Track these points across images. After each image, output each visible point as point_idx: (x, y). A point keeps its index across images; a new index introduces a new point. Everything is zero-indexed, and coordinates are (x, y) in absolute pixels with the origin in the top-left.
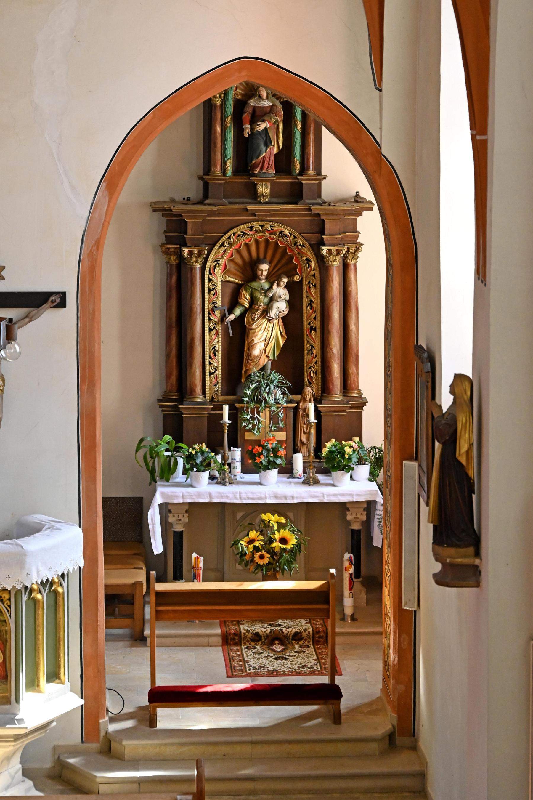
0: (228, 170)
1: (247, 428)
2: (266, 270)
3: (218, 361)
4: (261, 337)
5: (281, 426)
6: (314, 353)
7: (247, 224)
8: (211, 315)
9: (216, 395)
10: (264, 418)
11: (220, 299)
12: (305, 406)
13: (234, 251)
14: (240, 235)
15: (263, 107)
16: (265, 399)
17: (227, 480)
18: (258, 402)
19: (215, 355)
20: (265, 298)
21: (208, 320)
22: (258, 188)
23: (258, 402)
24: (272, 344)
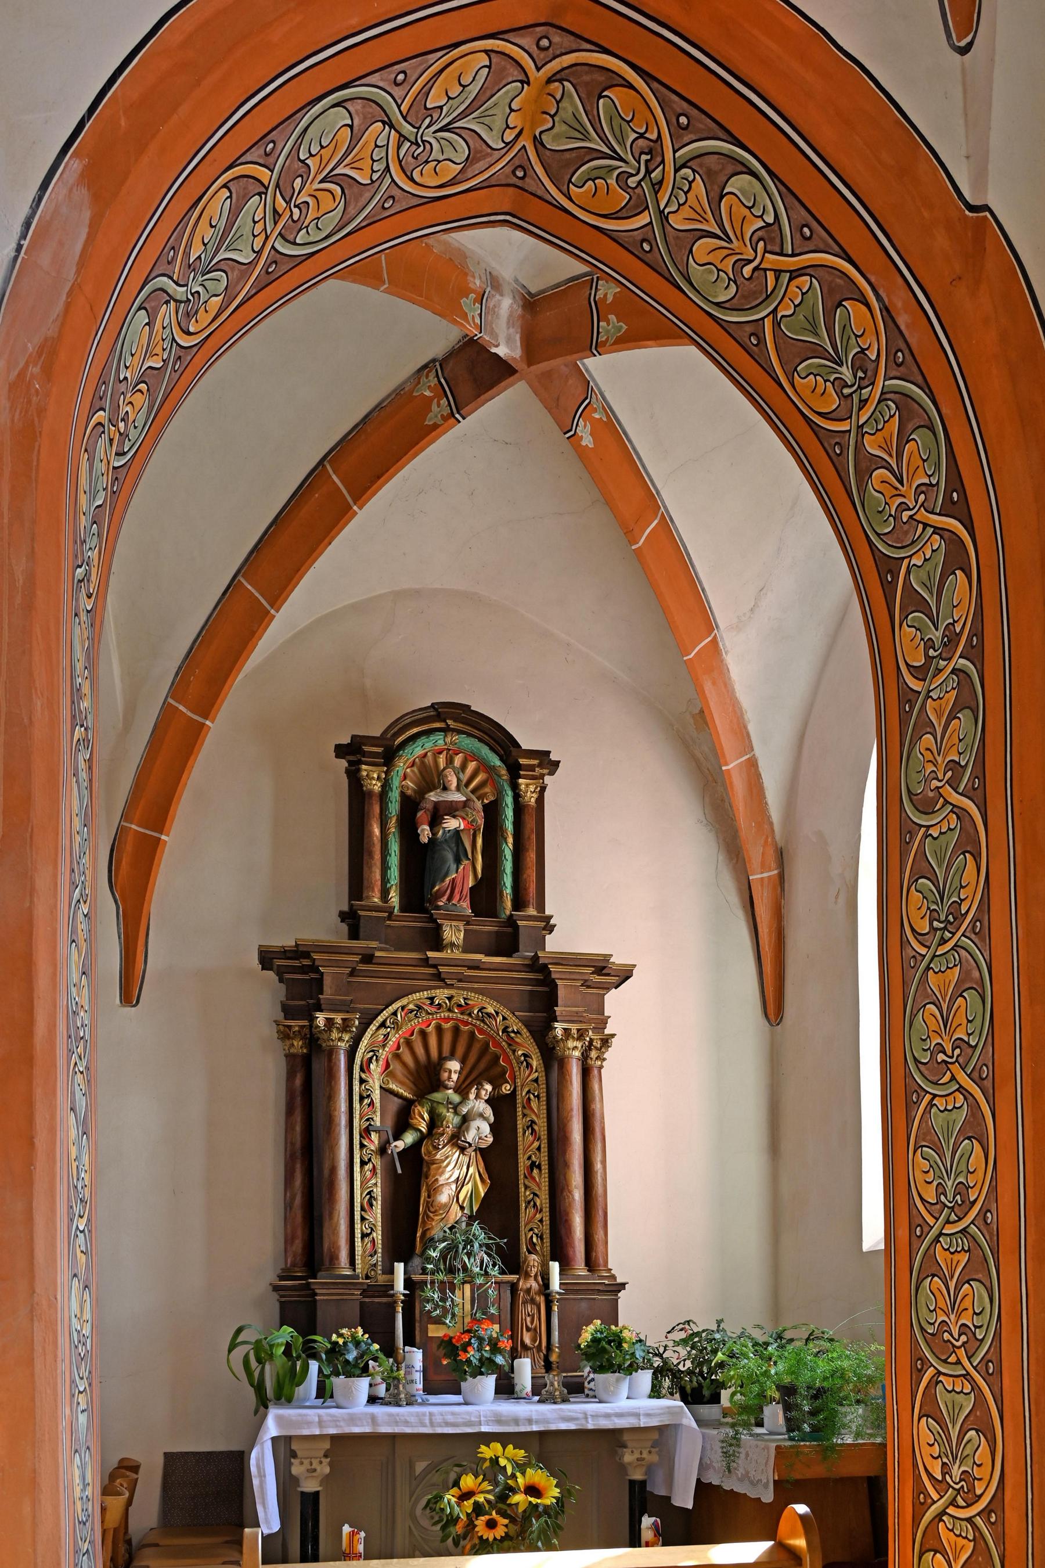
1: (434, 1314)
2: (455, 1072)
3: (376, 1214)
4: (451, 1176)
5: (492, 1311)
6: (538, 1204)
7: (425, 993)
8: (364, 1138)
9: (373, 1273)
10: (463, 1297)
11: (378, 1114)
12: (528, 1286)
13: (402, 1040)
14: (412, 1011)
16: (465, 1268)
17: (402, 1396)
18: (451, 1270)
19: (371, 1205)
21: (358, 1146)
23: (451, 1270)
24: (467, 1188)
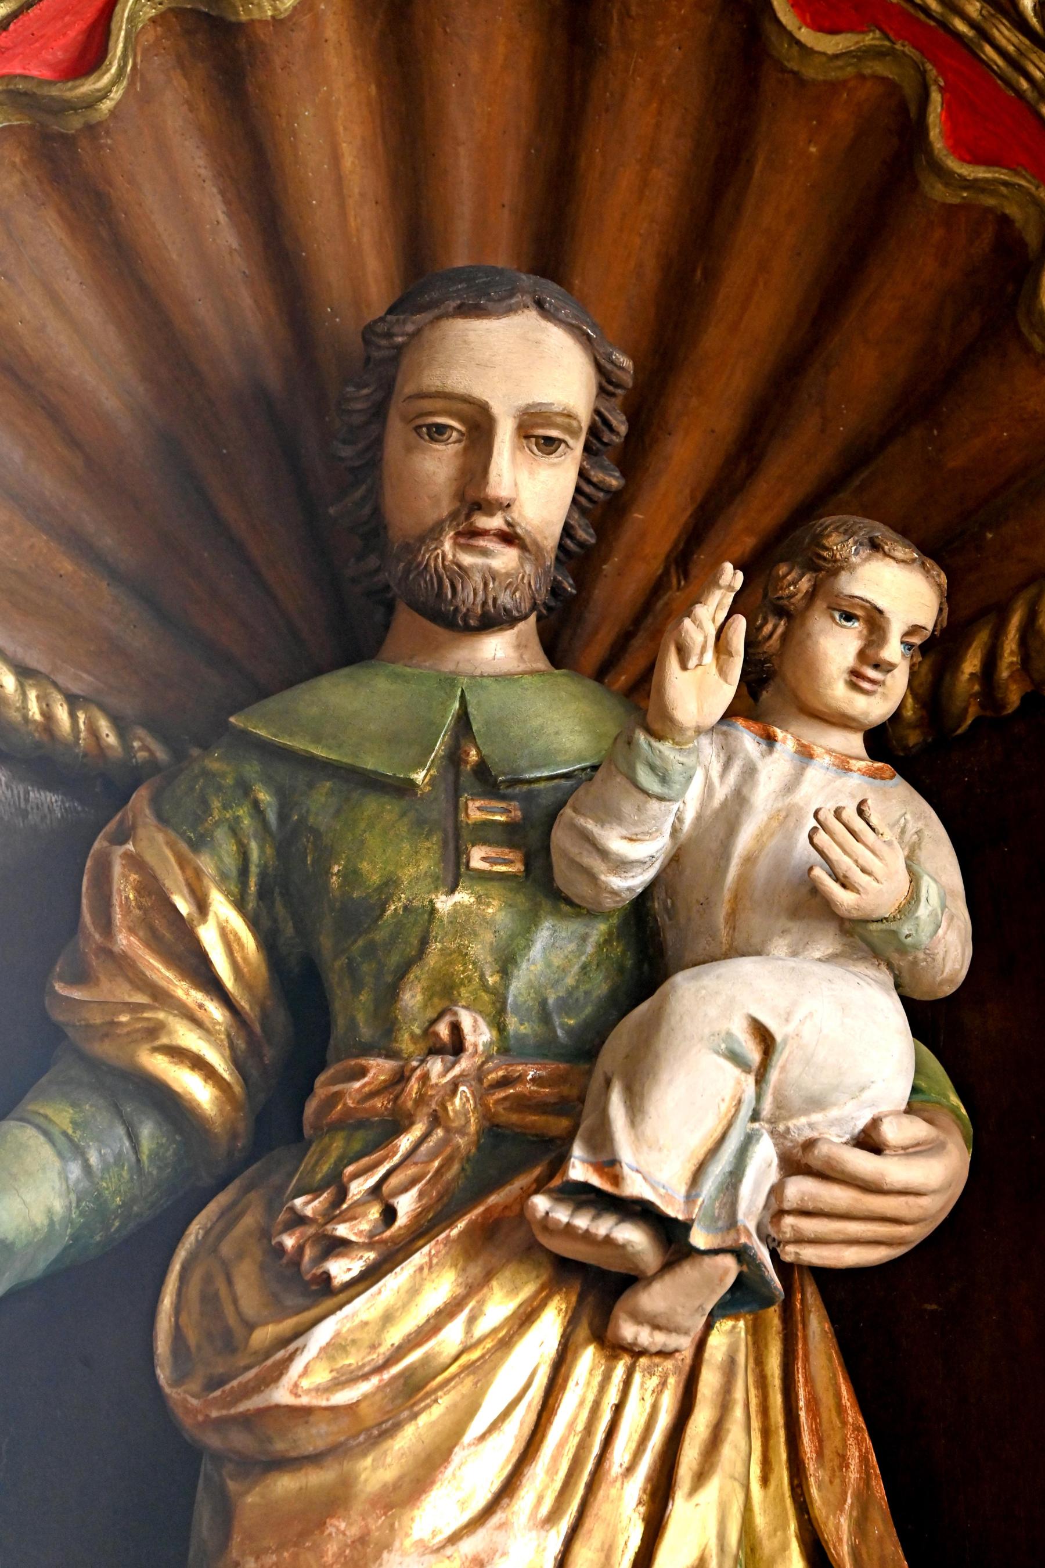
20: (529, 922)
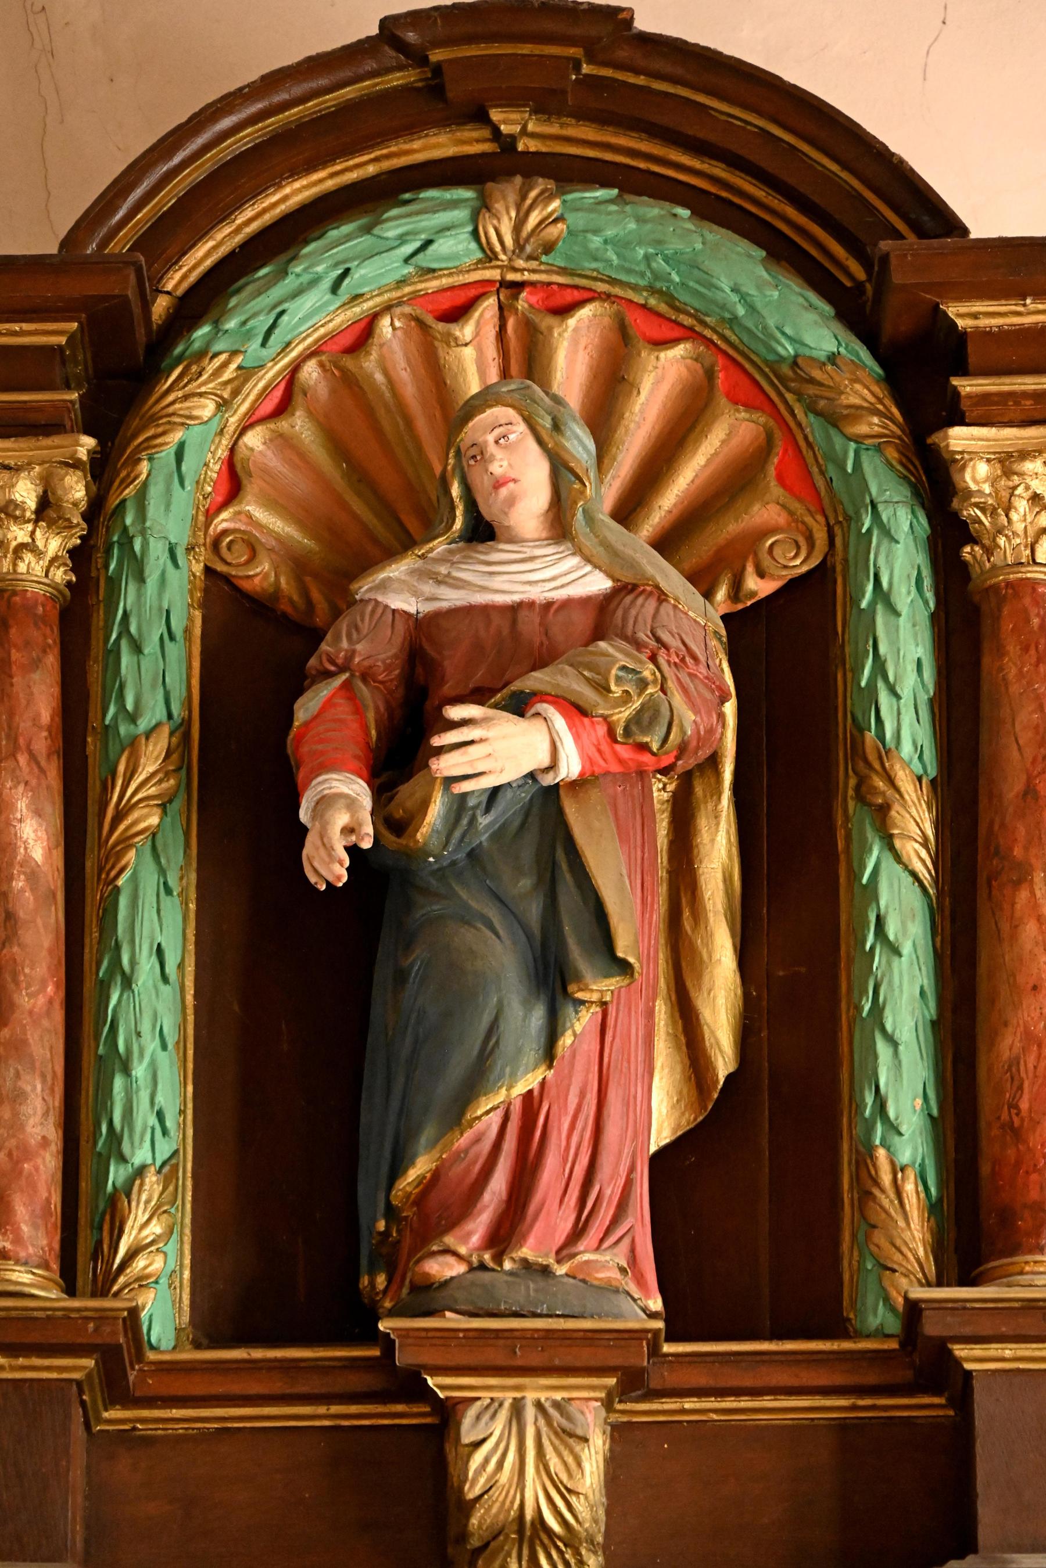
0: (142, 1282)
15: (514, 609)
22: (467, 1438)
